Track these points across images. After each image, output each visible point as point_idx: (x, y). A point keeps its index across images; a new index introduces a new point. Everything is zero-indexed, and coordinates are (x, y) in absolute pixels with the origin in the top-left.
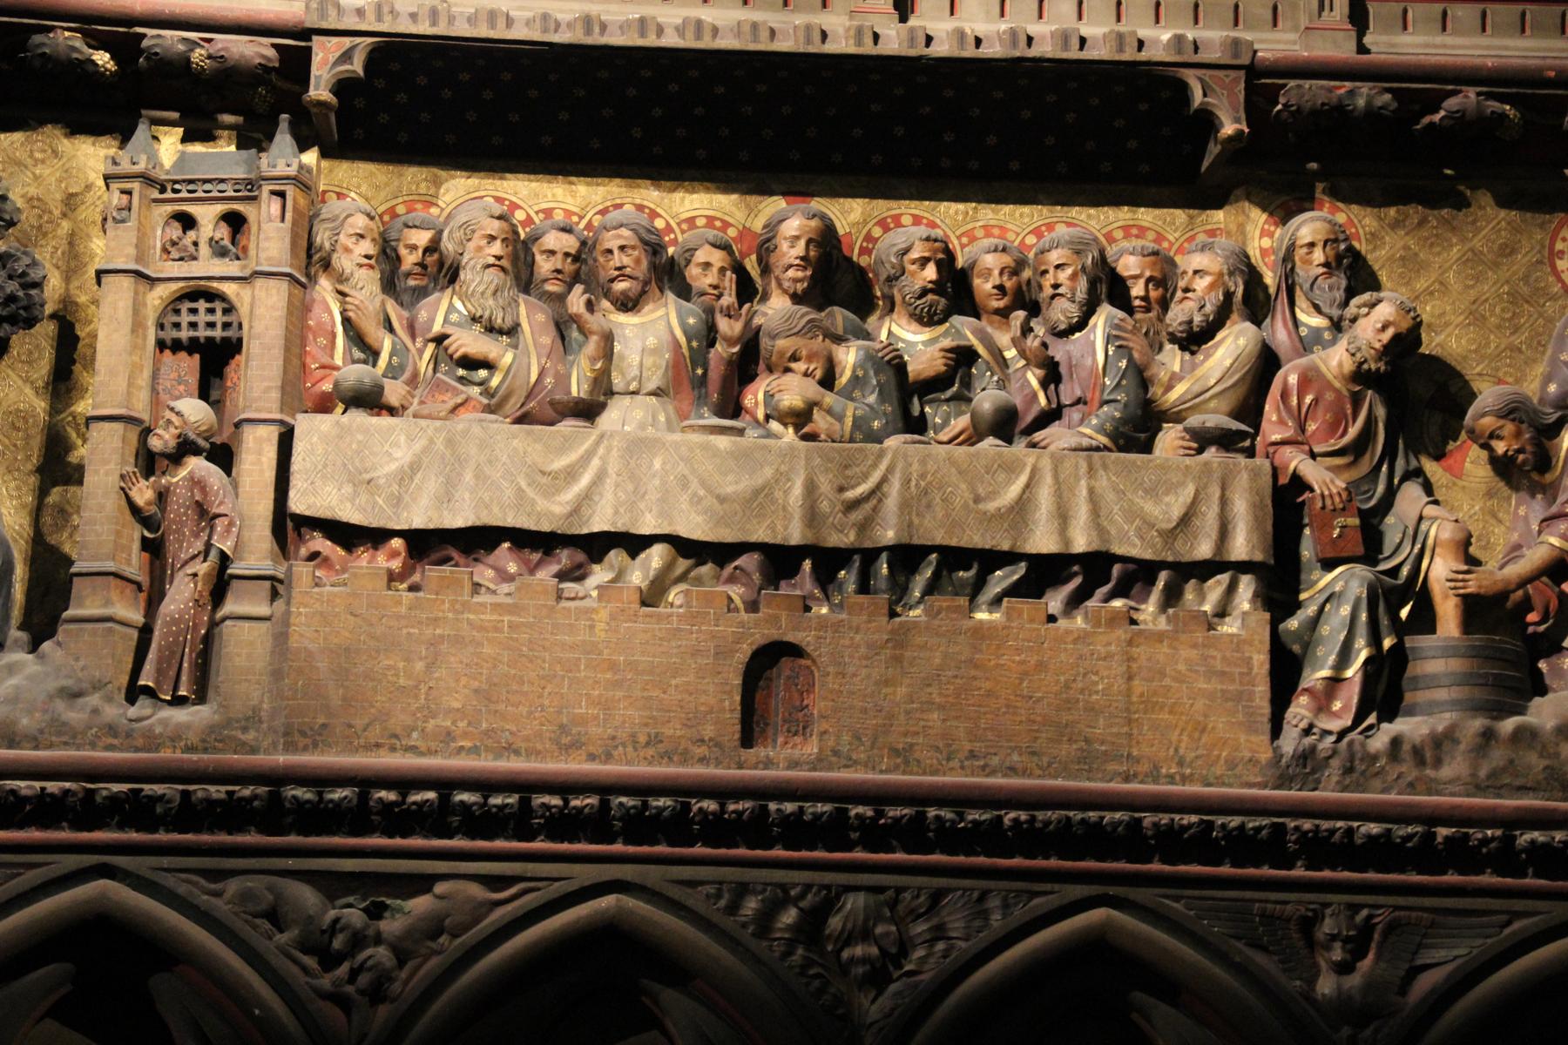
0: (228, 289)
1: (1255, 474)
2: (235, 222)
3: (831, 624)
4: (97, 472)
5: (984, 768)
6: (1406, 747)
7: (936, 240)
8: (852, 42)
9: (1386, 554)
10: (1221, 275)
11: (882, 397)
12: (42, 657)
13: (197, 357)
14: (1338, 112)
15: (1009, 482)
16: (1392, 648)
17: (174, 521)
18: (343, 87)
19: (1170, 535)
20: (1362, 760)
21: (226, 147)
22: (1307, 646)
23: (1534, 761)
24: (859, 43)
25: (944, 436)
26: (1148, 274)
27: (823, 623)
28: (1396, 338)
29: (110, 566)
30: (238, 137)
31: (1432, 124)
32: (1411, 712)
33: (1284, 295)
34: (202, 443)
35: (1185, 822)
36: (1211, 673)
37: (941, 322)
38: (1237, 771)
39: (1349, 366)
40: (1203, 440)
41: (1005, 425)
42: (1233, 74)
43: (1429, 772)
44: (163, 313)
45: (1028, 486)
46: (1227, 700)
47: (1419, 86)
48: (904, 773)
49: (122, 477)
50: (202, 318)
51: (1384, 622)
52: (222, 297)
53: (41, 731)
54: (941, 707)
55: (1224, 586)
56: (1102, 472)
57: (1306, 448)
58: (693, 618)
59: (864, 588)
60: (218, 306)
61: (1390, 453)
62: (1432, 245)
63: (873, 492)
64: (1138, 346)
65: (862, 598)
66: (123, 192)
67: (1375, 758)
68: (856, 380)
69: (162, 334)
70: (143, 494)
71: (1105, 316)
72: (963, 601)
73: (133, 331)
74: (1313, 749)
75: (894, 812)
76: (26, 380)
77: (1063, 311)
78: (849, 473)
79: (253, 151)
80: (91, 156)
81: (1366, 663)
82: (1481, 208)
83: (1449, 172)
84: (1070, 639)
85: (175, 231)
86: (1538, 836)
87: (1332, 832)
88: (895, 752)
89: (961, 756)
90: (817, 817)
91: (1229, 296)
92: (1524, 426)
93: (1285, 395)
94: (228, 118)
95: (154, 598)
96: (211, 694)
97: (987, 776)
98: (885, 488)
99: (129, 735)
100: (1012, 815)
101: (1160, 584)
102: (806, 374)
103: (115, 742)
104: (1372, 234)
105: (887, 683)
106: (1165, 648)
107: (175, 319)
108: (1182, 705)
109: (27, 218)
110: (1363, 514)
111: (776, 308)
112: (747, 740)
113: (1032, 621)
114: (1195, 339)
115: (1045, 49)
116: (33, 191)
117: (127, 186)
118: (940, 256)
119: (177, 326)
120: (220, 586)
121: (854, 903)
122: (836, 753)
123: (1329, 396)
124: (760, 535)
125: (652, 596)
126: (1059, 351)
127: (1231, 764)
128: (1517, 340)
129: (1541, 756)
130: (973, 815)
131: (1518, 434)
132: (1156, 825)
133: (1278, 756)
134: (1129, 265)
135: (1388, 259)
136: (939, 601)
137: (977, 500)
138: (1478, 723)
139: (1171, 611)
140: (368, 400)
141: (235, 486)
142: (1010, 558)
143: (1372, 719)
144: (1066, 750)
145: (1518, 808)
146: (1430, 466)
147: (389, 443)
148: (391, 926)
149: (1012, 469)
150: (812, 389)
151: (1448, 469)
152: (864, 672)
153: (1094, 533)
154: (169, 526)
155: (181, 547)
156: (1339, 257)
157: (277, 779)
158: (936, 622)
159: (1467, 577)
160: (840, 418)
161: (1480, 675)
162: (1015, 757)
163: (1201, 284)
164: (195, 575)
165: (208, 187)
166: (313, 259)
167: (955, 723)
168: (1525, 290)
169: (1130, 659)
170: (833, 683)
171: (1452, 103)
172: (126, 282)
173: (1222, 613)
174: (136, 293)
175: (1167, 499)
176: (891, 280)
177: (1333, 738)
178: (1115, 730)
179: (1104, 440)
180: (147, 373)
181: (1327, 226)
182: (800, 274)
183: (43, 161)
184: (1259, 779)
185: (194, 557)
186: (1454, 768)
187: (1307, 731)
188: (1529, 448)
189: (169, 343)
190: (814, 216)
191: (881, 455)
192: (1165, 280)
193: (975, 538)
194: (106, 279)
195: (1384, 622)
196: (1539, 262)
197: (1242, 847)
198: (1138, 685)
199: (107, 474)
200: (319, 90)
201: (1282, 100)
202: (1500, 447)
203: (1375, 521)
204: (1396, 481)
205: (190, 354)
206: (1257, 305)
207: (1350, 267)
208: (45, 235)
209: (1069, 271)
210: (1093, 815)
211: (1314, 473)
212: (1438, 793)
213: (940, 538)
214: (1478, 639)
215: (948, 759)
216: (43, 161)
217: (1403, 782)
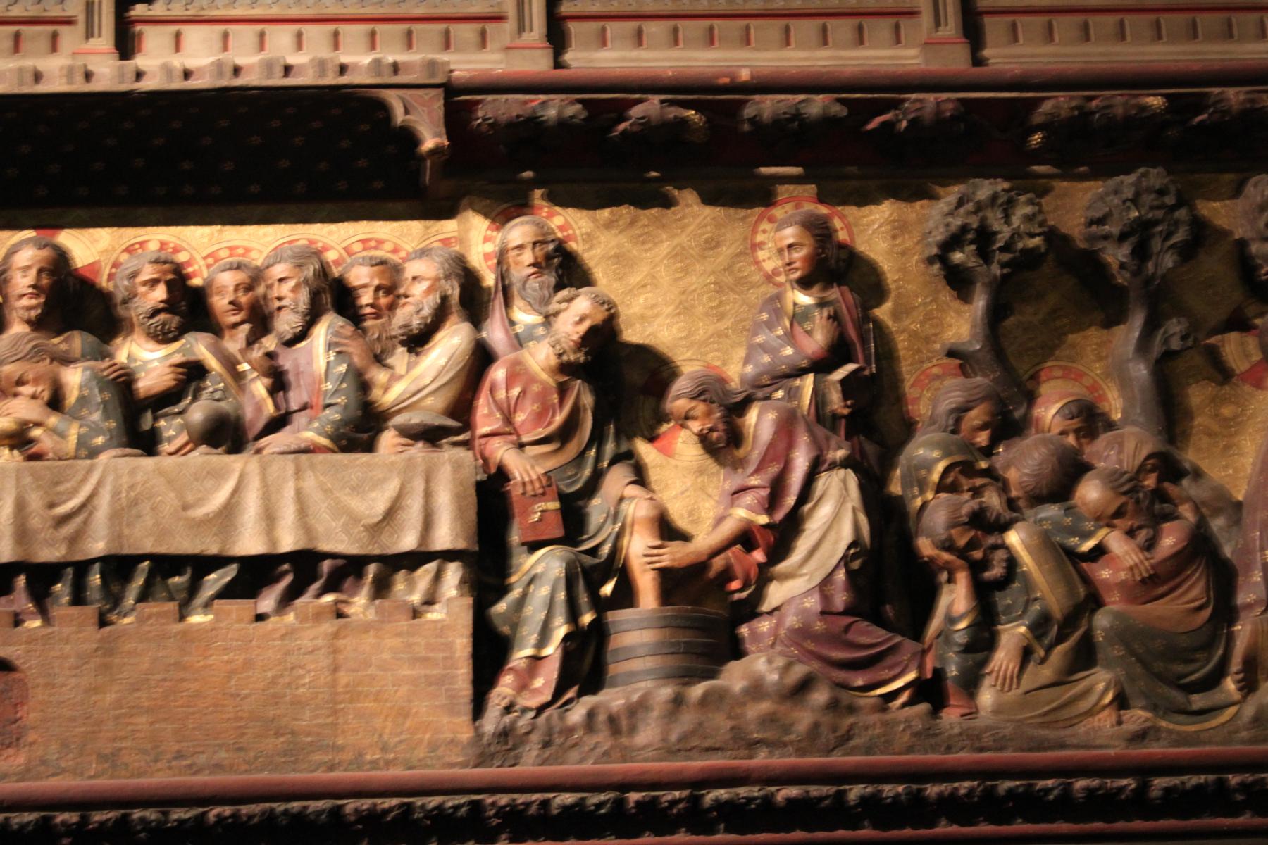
1: (457, 466)
5: (190, 766)
6: (602, 717)
7: (165, 262)
8: (64, 80)
9: (591, 533)
10: (437, 279)
11: (106, 416)
15: (217, 488)
16: (593, 622)
20: (560, 732)
22: (515, 626)
23: (721, 723)
24: (70, 82)
25: (172, 448)
26: (376, 282)
27: (32, 638)
28: (592, 331)
31: (624, 132)
32: (613, 685)
33: (500, 295)
35: (386, 805)
36: (416, 660)
37: (175, 339)
38: (440, 752)
39: (554, 361)
41: (226, 434)
42: (433, 92)
43: (624, 740)
45: (236, 491)
46: (430, 684)
47: (606, 99)
48: (112, 777)
51: (584, 598)
54: (149, 711)
55: (432, 574)
56: (309, 473)
57: (514, 438)
59: (78, 598)
61: (597, 438)
62: (644, 243)
63: (83, 506)
64: (356, 351)
65: (76, 610)
67: (571, 730)
68: (83, 400)
72: (172, 606)
74: (514, 722)
75: (98, 817)
77: (287, 323)
78: (61, 488)
81: (566, 638)
82: (688, 206)
83: (654, 174)
84: (277, 635)
86: (723, 794)
87: (528, 805)
88: (102, 758)
89: (169, 756)
90: (23, 826)
91: (445, 299)
92: (715, 405)
93: (492, 390)
97: (195, 773)
98: (96, 502)
100: (217, 810)
101: (370, 577)
102: (34, 397)
104: (588, 234)
105: (94, 689)
106: (369, 639)
108: (388, 693)
110: (563, 497)
113: (240, 620)
114: (417, 341)
118: (170, 277)
122: (43, 762)
123: (536, 388)
126: (287, 361)
127: (433, 747)
128: (722, 325)
129: (729, 717)
130: (178, 814)
131: (708, 414)
132: (356, 810)
133: (479, 735)
135: (603, 257)
136: (150, 608)
137: (186, 507)
138: (666, 692)
139: (377, 602)
142: (218, 562)
143: (571, 694)
144: (272, 744)
145: (702, 769)
146: (644, 449)
149: (218, 475)
151: (661, 450)
152: (73, 681)
153: (301, 532)
156: (548, 257)
158: (147, 628)
159: (661, 551)
160: (62, 435)
161: (673, 644)
162: (223, 754)
163: (418, 290)
167: (163, 725)
168: (728, 279)
169: (336, 651)
170: (39, 695)
171: (636, 112)
173: (430, 601)
175: (373, 495)
176: (125, 302)
177: (532, 714)
178: (320, 721)
179: (324, 441)
181: (534, 228)
182: (34, 302)
184: (461, 759)
186: (648, 734)
187: (508, 709)
188: (721, 426)
190: (45, 246)
191: (90, 471)
192: (391, 288)
193: (184, 544)
195: (584, 598)
196: (742, 253)
198: (344, 678)
201: (480, 114)
202: (695, 426)
203: (581, 503)
204: (605, 464)
207: (561, 266)
209: (292, 283)
210: (295, 806)
212: (632, 760)
213: (148, 546)
214: (670, 610)
215: (156, 761)
217: (599, 751)
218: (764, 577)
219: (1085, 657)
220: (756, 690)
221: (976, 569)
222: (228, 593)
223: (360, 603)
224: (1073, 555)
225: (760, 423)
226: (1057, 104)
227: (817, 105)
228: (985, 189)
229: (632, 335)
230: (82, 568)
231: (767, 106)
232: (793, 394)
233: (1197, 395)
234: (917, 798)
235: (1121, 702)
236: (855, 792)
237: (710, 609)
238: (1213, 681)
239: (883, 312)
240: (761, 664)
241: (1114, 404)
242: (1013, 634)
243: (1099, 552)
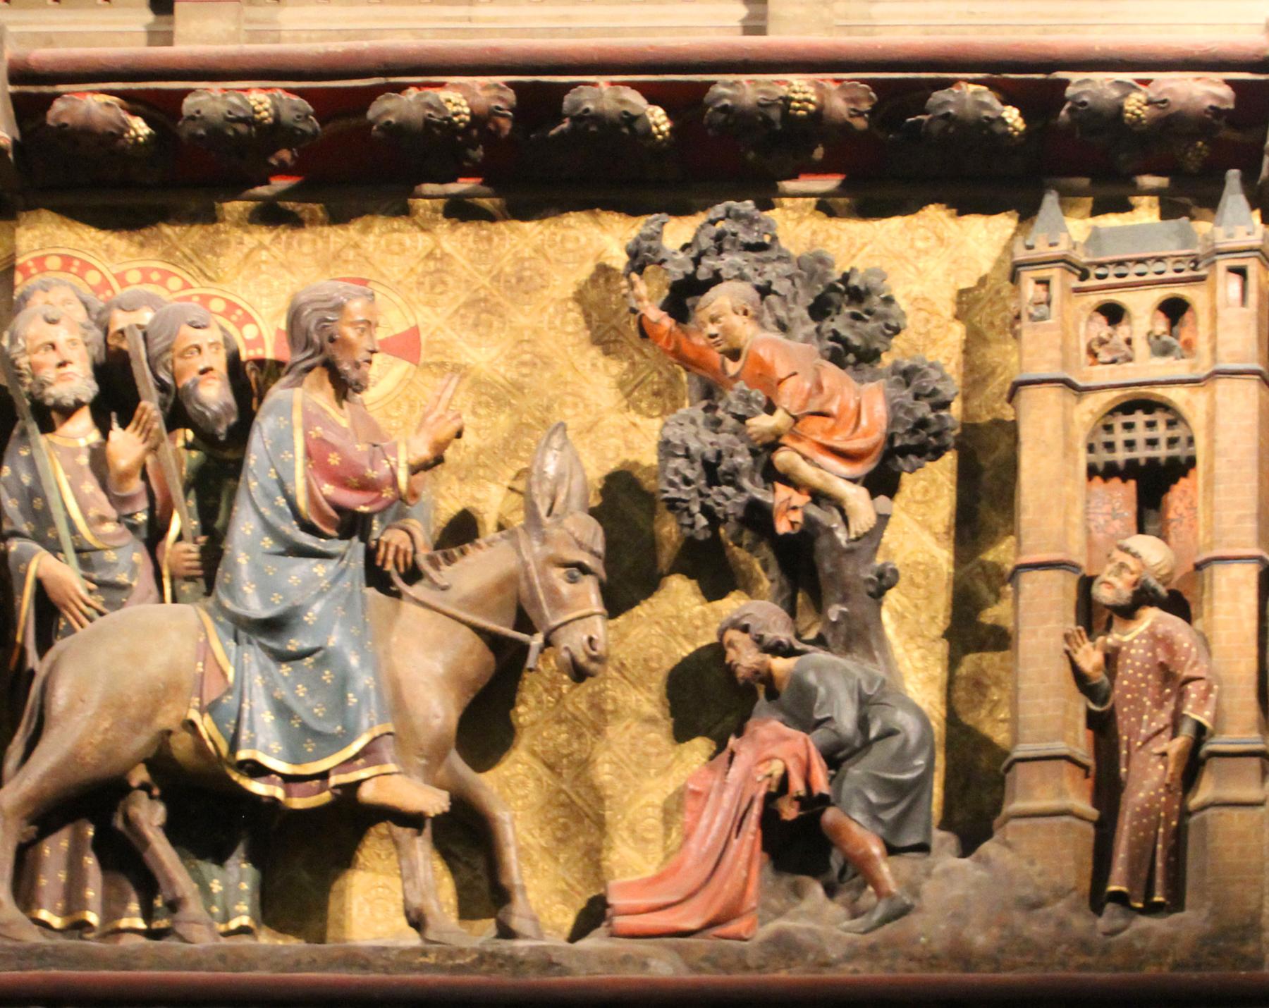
0: (1176, 395)
4: (1034, 633)
12: (986, 862)
13: (1132, 484)
17: (1127, 690)
29: (1060, 747)
30: (1161, 203)
34: (1162, 590)
44: (1093, 433)
49: (1067, 637)
50: (1140, 434)
52: (1165, 407)
53: (1001, 950)
60: (1160, 417)
66: (1039, 282)
69: (1093, 458)
70: (1090, 658)
73: (1065, 455)
76: (926, 526)
79: (1184, 220)
85: (1100, 327)
94: (1149, 181)
96: (1190, 898)
99: (1106, 951)
103: (1090, 960)
107: (1106, 437)
109: (913, 324)
116: (916, 289)
117: (1043, 273)
119: (1110, 446)
120: (1192, 767)
141: (1205, 641)
154: (1123, 697)
155: (1140, 722)
164: (1164, 754)
165: (1141, 268)
172: (1052, 394)
174: (1065, 406)
180: (1079, 507)
183: (926, 252)
185: (1159, 732)
189: (1101, 467)
194: (1027, 393)
199: (1047, 635)
205: (1124, 480)
208: (934, 342)
216: (926, 252)
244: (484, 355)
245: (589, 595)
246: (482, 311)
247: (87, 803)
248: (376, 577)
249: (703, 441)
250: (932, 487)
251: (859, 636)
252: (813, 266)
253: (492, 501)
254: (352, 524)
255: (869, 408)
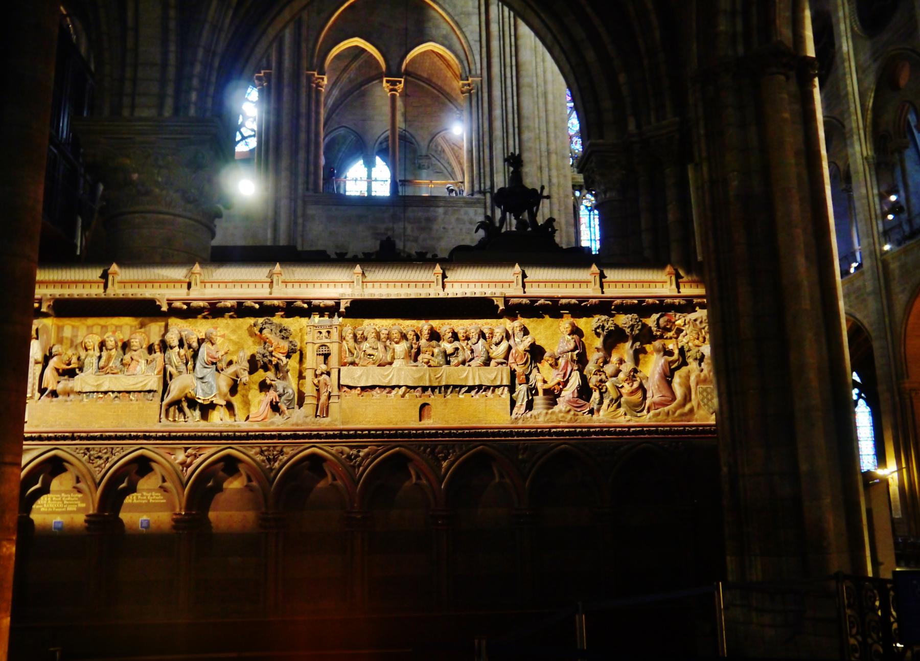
2: (329, 332)
3: (434, 399)
14: (520, 304)
18: (346, 308)
19: (492, 381)
21: (326, 318)
23: (554, 417)
40: (499, 363)
41: (464, 363)
47: (534, 300)
58: (410, 399)
61: (531, 363)
70: (316, 381)
71: (482, 341)
77: (474, 340)
80: (304, 321)
95: (318, 399)
109: (294, 333)
111: (423, 342)
112: (420, 420)
114: (497, 344)
115: (468, 295)
120: (329, 397)
121: (440, 447)
124: (421, 384)
125: (403, 396)
126: (473, 347)
134: (486, 331)
140: (353, 363)
142: (465, 386)
144: (476, 419)
147: (357, 371)
148: (361, 454)
149: (465, 371)
150: (429, 357)
157: (341, 430)
166: (342, 338)
186: (541, 419)
197: (506, 434)
200: (342, 309)
206: (508, 337)
211: (517, 368)
218: (561, 390)
219: (619, 406)
220: (560, 412)
221: (600, 390)
222: (466, 392)
223: (489, 393)
224: (617, 387)
225: (562, 362)
226: (618, 301)
227: (574, 301)
228: (604, 317)
229: (537, 343)
230: (440, 387)
231: (563, 301)
232: (567, 356)
233: (641, 356)
234: (589, 431)
235: (625, 414)
236: (578, 430)
237: (552, 396)
238: (642, 411)
239: (583, 339)
240: (562, 405)
241: (626, 358)
242: (606, 402)
243: (623, 387)
244: (234, 337)
245: (246, 373)
246: (234, 331)
247: (177, 403)
248: (217, 370)
249: (262, 351)
250: (296, 356)
251: (284, 378)
252: (280, 325)
253: (235, 358)
254: (213, 363)
255: (285, 345)
